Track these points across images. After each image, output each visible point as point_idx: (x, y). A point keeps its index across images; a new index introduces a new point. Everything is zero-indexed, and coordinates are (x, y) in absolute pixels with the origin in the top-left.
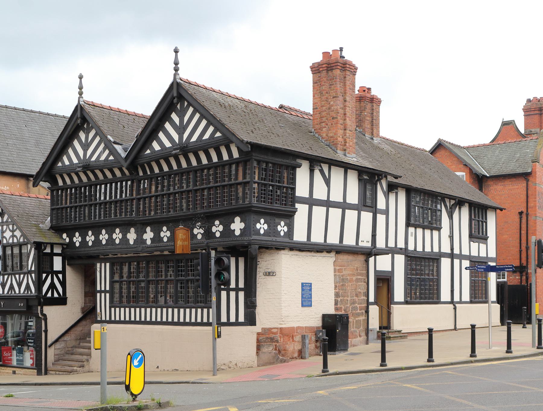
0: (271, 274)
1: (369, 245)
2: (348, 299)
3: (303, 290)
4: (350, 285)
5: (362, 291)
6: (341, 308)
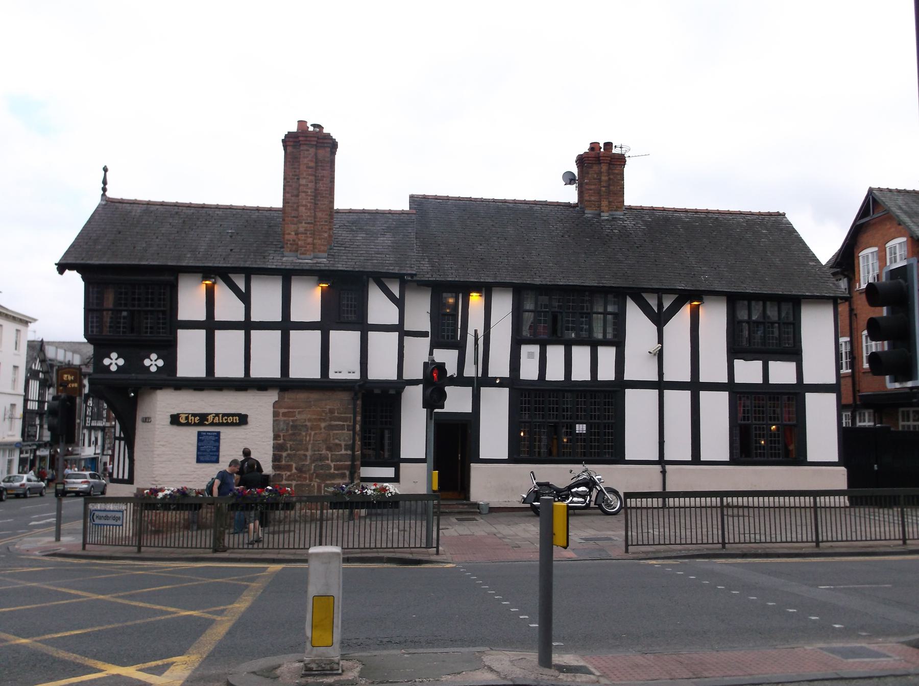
0: (147, 420)
1: (357, 376)
2: (306, 453)
3: (199, 440)
4: (312, 435)
5: (343, 443)
6: (291, 466)
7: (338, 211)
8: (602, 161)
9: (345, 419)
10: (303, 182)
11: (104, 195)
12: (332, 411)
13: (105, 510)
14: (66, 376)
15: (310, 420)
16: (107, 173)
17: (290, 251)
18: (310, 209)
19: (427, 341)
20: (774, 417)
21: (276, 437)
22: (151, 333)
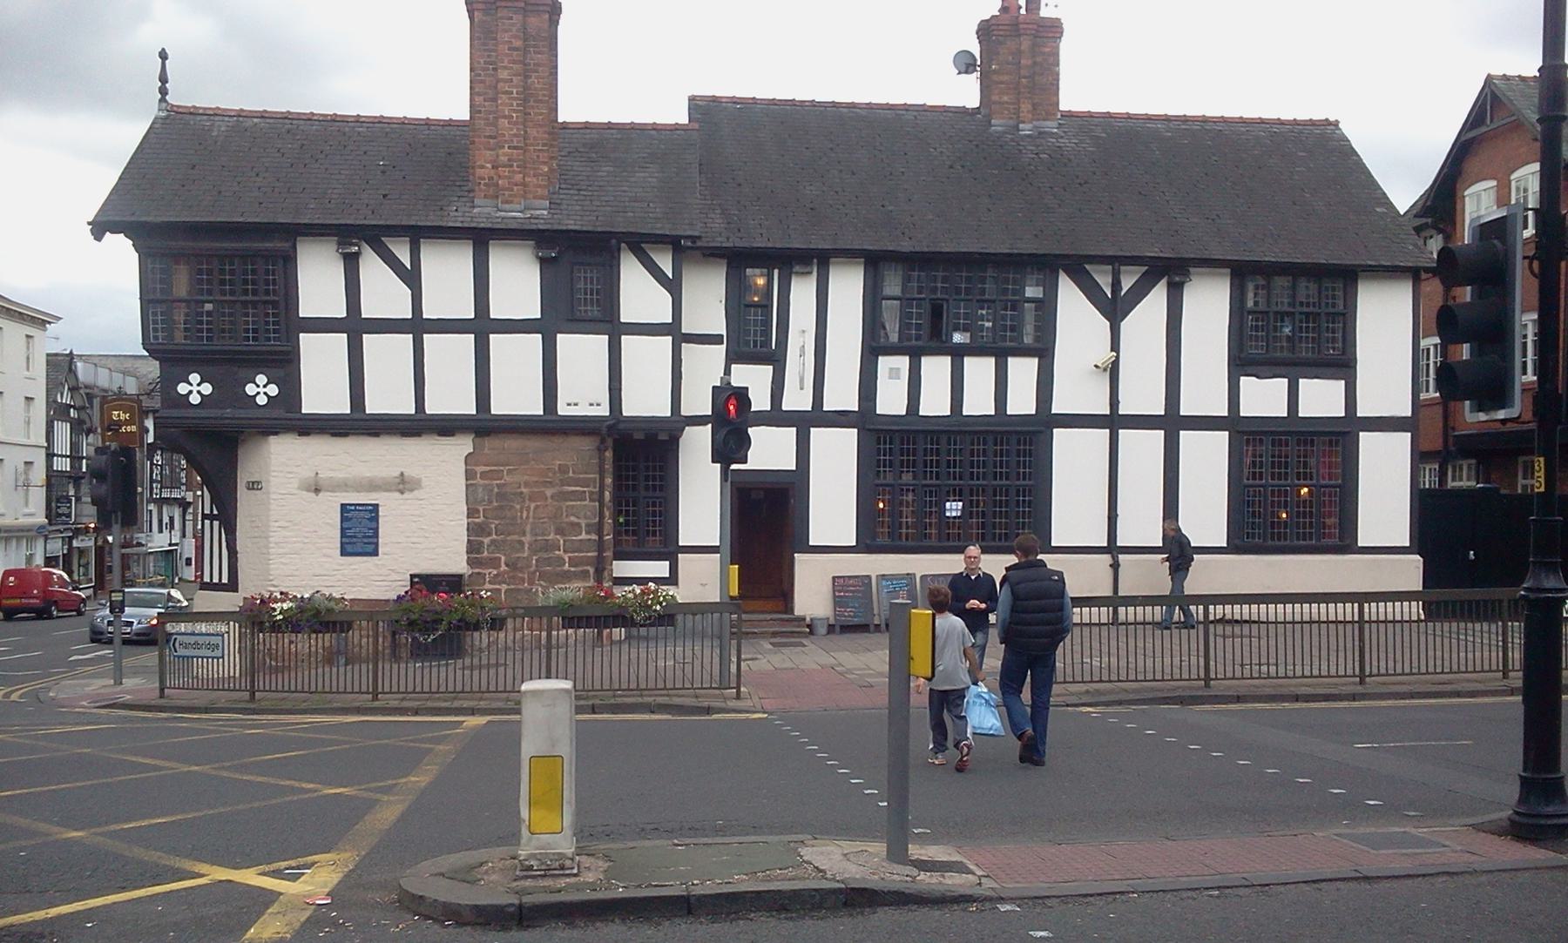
1: (604, 411)
2: (523, 539)
3: (343, 519)
4: (532, 508)
6: (500, 558)
7: (565, 126)
8: (1022, 31)
9: (585, 483)
10: (503, 74)
11: (163, 100)
12: (563, 469)
13: (193, 634)
14: (116, 413)
15: (527, 484)
16: (167, 62)
17: (485, 196)
18: (516, 123)
19: (721, 349)
20: (1305, 473)
21: (471, 513)
22: (255, 339)
